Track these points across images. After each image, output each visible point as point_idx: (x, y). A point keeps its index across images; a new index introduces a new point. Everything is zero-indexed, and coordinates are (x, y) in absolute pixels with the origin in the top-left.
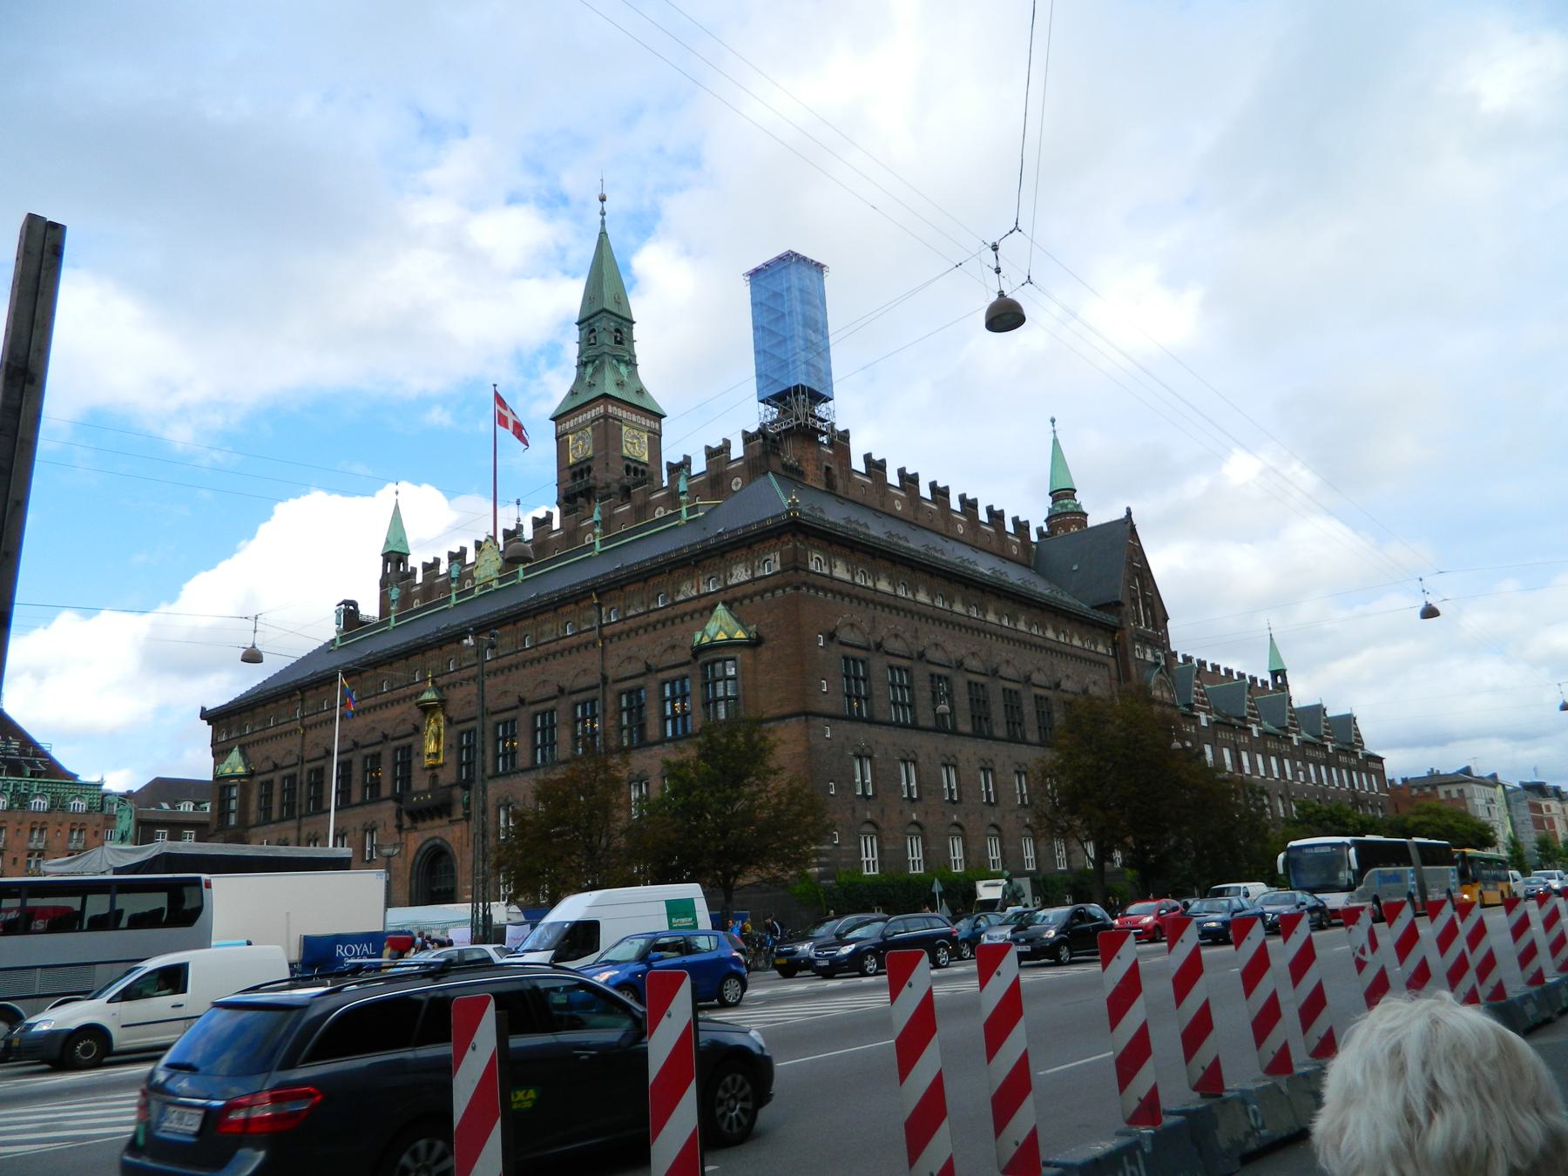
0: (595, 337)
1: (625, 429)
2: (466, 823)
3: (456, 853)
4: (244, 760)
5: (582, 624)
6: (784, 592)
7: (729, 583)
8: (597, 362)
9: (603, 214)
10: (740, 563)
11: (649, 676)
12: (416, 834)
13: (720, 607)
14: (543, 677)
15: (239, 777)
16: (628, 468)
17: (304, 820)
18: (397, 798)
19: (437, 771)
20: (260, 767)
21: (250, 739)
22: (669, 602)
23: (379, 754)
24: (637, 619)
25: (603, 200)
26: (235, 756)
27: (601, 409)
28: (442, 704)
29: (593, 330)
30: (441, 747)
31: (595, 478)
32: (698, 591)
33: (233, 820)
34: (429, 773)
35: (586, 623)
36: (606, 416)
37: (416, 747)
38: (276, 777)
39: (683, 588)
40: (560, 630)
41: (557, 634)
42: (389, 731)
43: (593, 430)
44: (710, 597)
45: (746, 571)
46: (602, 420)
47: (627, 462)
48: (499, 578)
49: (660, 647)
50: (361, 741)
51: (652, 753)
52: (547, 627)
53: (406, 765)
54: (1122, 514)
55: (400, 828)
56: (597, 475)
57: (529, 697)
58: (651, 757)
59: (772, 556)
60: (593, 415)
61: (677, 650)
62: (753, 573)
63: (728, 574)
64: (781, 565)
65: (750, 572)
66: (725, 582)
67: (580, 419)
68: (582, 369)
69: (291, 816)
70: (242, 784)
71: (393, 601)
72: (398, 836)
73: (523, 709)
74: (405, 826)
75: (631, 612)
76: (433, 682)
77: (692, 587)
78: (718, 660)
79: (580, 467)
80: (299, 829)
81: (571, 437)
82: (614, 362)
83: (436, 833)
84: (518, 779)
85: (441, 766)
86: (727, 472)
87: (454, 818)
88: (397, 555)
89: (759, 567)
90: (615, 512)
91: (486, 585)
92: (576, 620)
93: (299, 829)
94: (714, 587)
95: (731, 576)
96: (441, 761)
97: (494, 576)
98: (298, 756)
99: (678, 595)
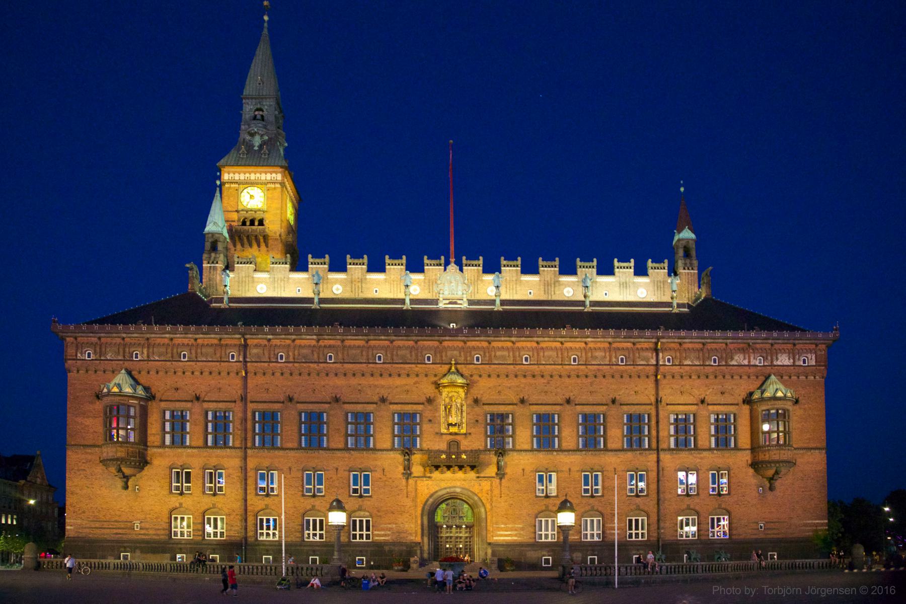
2: (498, 481)
5: (638, 360)
6: (815, 377)
7: (775, 363)
10: (785, 353)
14: (591, 389)
19: (458, 438)
22: (724, 363)
24: (693, 368)
30: (464, 420)
32: (749, 362)
35: (642, 360)
37: (428, 414)
38: (197, 407)
39: (736, 358)
40: (614, 360)
44: (759, 368)
45: (789, 359)
59: (809, 356)
61: (726, 395)
62: (794, 362)
63: (775, 358)
64: (816, 362)
65: (792, 361)
66: (772, 362)
72: (404, 481)
73: (568, 407)
74: (415, 474)
75: (688, 362)
76: (456, 369)
77: (745, 359)
80: (245, 458)
83: (458, 484)
84: (562, 456)
85: (465, 434)
87: (482, 475)
89: (799, 359)
92: (631, 355)
93: (245, 458)
94: (760, 363)
95: (777, 359)
96: (464, 431)
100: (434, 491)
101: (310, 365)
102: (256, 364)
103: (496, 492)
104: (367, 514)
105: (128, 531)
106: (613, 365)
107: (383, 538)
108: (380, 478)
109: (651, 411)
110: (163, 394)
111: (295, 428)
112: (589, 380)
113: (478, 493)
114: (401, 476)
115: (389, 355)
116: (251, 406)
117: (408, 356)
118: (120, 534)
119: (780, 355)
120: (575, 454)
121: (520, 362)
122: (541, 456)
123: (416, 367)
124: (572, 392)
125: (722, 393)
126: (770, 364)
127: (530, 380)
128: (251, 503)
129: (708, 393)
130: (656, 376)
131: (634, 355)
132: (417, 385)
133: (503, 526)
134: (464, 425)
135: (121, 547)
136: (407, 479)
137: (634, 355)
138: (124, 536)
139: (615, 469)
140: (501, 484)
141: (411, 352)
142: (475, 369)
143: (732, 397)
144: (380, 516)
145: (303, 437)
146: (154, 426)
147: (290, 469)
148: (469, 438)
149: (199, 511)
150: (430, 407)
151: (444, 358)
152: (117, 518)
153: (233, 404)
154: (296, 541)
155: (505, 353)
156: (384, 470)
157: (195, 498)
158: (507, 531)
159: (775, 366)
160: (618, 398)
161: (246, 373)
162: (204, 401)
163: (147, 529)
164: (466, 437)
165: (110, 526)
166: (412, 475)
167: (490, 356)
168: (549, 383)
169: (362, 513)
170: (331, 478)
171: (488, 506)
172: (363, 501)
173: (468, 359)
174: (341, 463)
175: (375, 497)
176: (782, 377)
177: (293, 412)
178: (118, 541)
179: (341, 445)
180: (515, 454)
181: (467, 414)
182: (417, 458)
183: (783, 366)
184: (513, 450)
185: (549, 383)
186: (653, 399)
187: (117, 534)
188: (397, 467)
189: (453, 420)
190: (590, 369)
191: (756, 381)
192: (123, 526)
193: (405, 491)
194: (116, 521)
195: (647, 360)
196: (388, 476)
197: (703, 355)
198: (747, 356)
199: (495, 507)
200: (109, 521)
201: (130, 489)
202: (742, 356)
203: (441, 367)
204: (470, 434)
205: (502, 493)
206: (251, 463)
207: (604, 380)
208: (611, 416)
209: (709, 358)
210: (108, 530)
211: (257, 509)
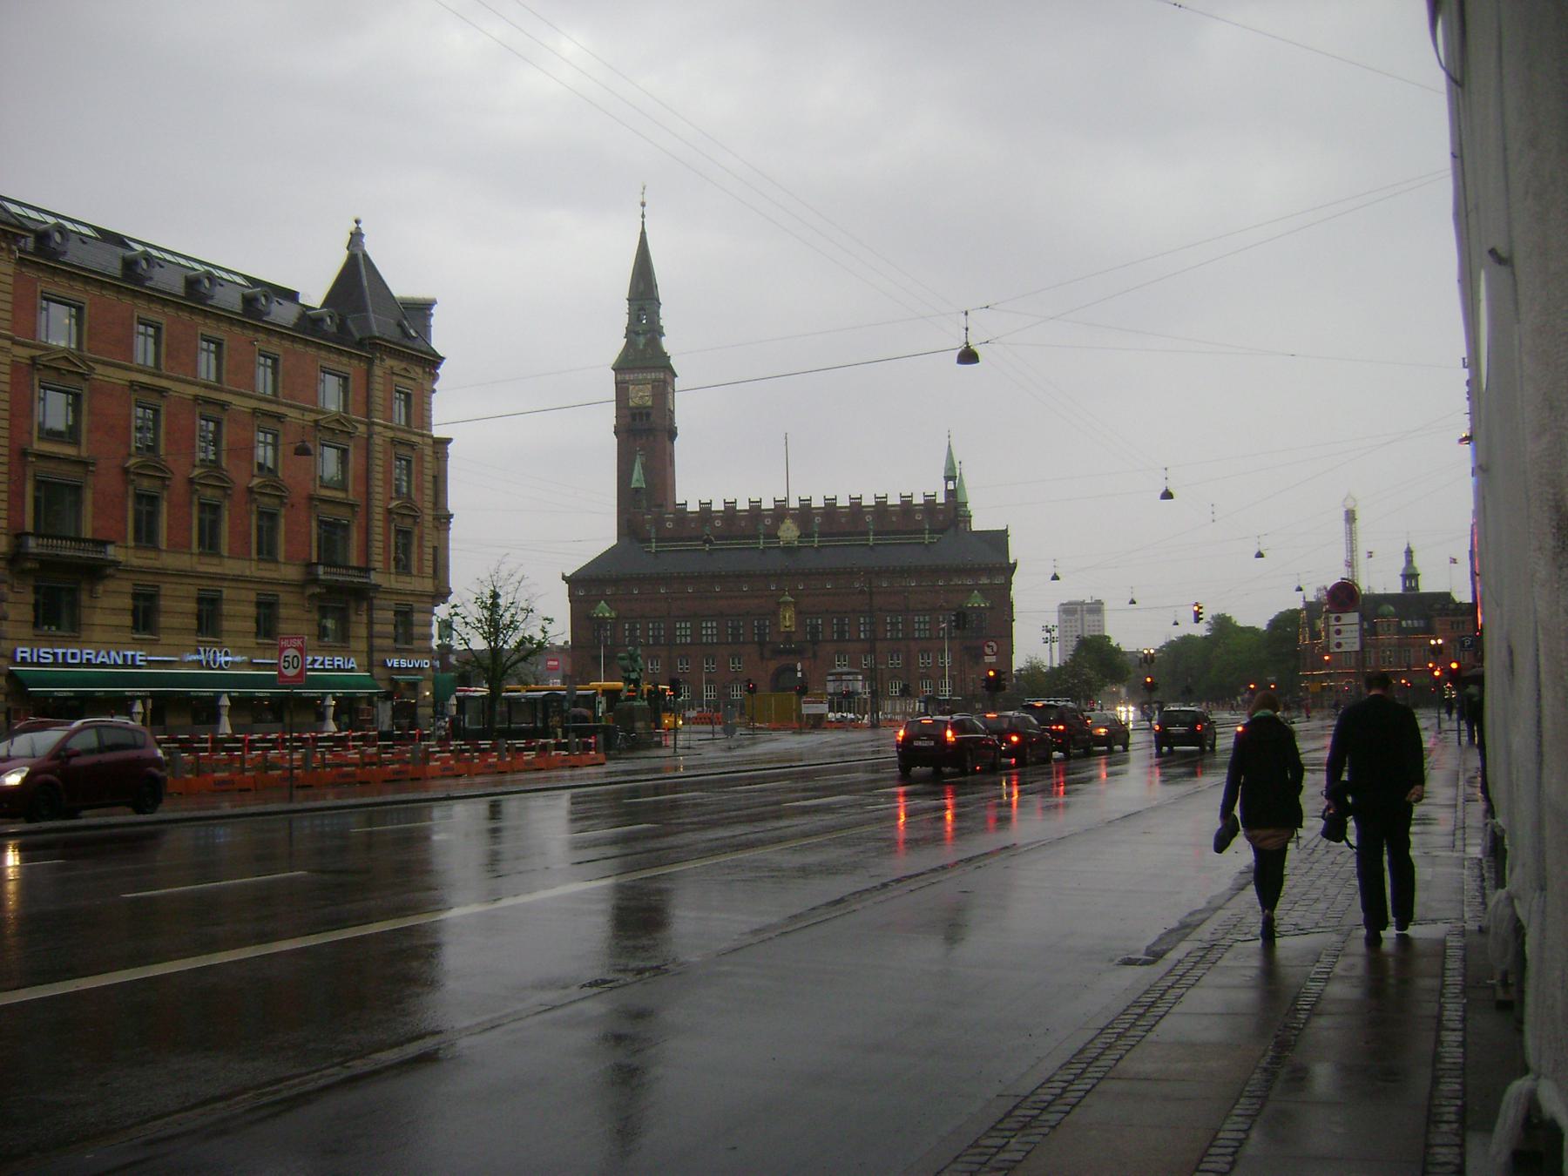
9: (643, 216)
15: (612, 618)
25: (643, 205)
26: (603, 602)
27: (662, 376)
43: (653, 388)
46: (661, 383)
54: (1004, 528)
55: (762, 657)
60: (654, 377)
67: (640, 376)
68: (633, 335)
75: (924, 584)
81: (631, 387)
85: (794, 632)
183: (983, 584)
189: (788, 624)
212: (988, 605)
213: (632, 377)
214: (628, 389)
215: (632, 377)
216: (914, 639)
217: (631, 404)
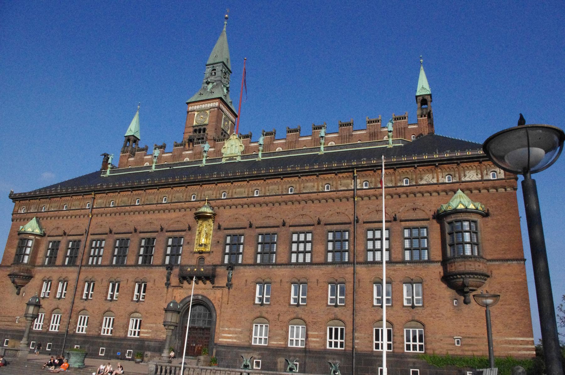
0: (215, 73)
1: (224, 116)
2: (227, 290)
3: (216, 307)
4: (39, 226)
7: (463, 179)
8: (215, 84)
10: (472, 169)
11: (394, 223)
12: (182, 291)
13: (459, 191)
14: (302, 213)
16: (222, 133)
17: (83, 268)
18: (170, 267)
19: (204, 255)
20: (51, 232)
21: (46, 214)
22: (414, 183)
23: (59, 242)
26: (33, 222)
27: (217, 104)
28: (214, 216)
29: (215, 70)
31: (207, 134)
32: (438, 180)
33: (26, 259)
34: (198, 255)
35: (343, 186)
36: (219, 108)
38: (63, 240)
39: (425, 177)
40: (320, 188)
41: (318, 189)
42: (166, 227)
43: (210, 112)
44: (448, 185)
47: (223, 131)
48: (241, 156)
49: (404, 207)
50: (139, 229)
51: (395, 268)
52: (310, 184)
53: (176, 246)
55: (168, 285)
56: (209, 133)
57: (289, 222)
58: (394, 270)
61: (417, 211)
62: (482, 177)
63: (462, 175)
65: (480, 176)
66: (460, 179)
67: (203, 106)
68: (206, 85)
69: (72, 263)
70: (36, 239)
71: (155, 156)
76: (208, 203)
78: (457, 221)
79: (199, 127)
81: (196, 113)
82: (223, 86)
84: (276, 269)
85: (209, 252)
86: (381, 132)
88: (134, 138)
89: (487, 174)
90: (299, 139)
91: (231, 158)
92: (334, 183)
94: (449, 180)
95: (465, 176)
96: (208, 249)
97: (238, 154)
98: (86, 230)
99: (421, 181)
100: (183, 297)
101: (126, 207)
102: (98, 209)
103: (225, 299)
104: (140, 315)
105: (13, 324)
106: (319, 192)
107: (146, 335)
108: (152, 287)
109: (350, 228)
110: (51, 232)
111: (111, 251)
112: (301, 206)
113: (213, 300)
114: (164, 286)
115: (170, 197)
116: (90, 237)
117: (181, 196)
118: (8, 325)
119: (467, 172)
120: (287, 268)
121: (252, 195)
122: (260, 269)
123: (185, 204)
124: (287, 215)
125: (414, 209)
126: (458, 180)
127: (258, 208)
128: (77, 304)
129: (400, 211)
130: (354, 199)
131: (337, 183)
132: (184, 217)
133: (227, 329)
134: (209, 246)
135: (6, 334)
136: (168, 288)
137: (337, 183)
138: (10, 327)
139: (318, 280)
140: (229, 292)
141: (183, 194)
142: (222, 202)
143: (424, 213)
144: (147, 317)
145: (115, 258)
146: (42, 252)
147: (102, 280)
148: (212, 255)
149: (50, 310)
150: (190, 233)
151: (203, 196)
152: (9, 315)
153: (82, 237)
154: (95, 335)
155: (242, 190)
156: (155, 280)
157: (50, 301)
158: (229, 334)
159: (463, 182)
160: (322, 219)
161: (92, 216)
162: (69, 235)
163: (22, 322)
164: (209, 255)
165: (5, 320)
166: (172, 285)
167: (232, 192)
168: (271, 210)
169: (138, 314)
170: (123, 287)
171: (218, 312)
172: (139, 305)
173: (218, 195)
174: (131, 275)
175: (146, 301)
176: (471, 192)
177: (112, 240)
178: (6, 331)
179: (133, 263)
180: (242, 267)
181: (213, 236)
182: (176, 271)
184: (241, 265)
185: (271, 210)
186: (352, 218)
187: (6, 325)
188: (163, 278)
189: (203, 241)
190: (301, 197)
191: (445, 197)
192: (11, 320)
193: (165, 297)
194: (9, 317)
195: (348, 185)
196: (156, 286)
197: (395, 178)
198: (435, 175)
199: (223, 312)
200: (5, 316)
201: (20, 295)
202: (430, 176)
203: (200, 203)
204: (213, 252)
205: (229, 300)
206: (82, 276)
207: (313, 205)
208: (317, 234)
209: (401, 180)
210: (4, 323)
211: (79, 309)
212: (480, 208)
213: (198, 107)
214: (194, 115)
215: (198, 107)
216: (366, 263)
217: (195, 124)
